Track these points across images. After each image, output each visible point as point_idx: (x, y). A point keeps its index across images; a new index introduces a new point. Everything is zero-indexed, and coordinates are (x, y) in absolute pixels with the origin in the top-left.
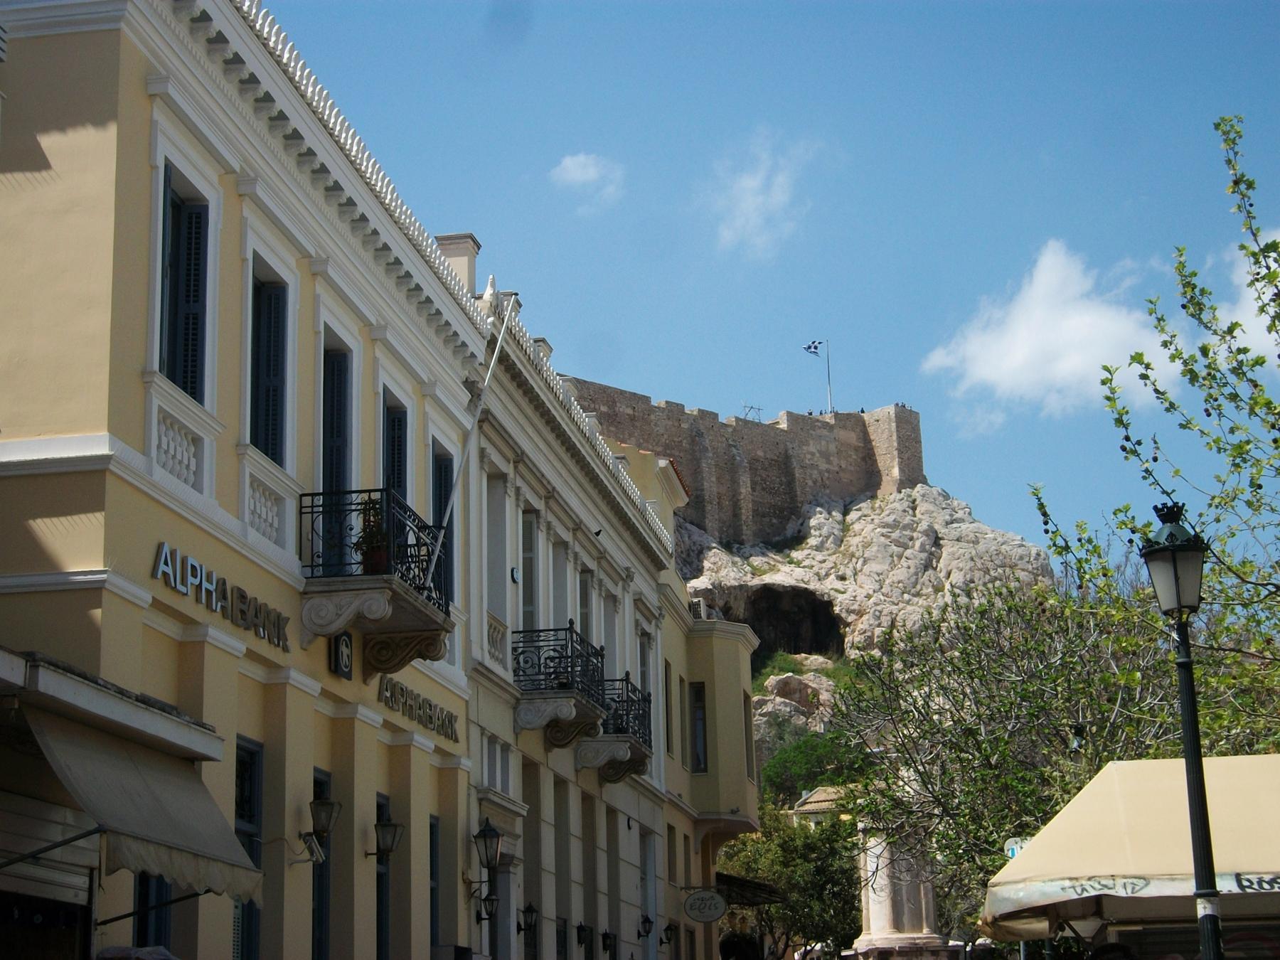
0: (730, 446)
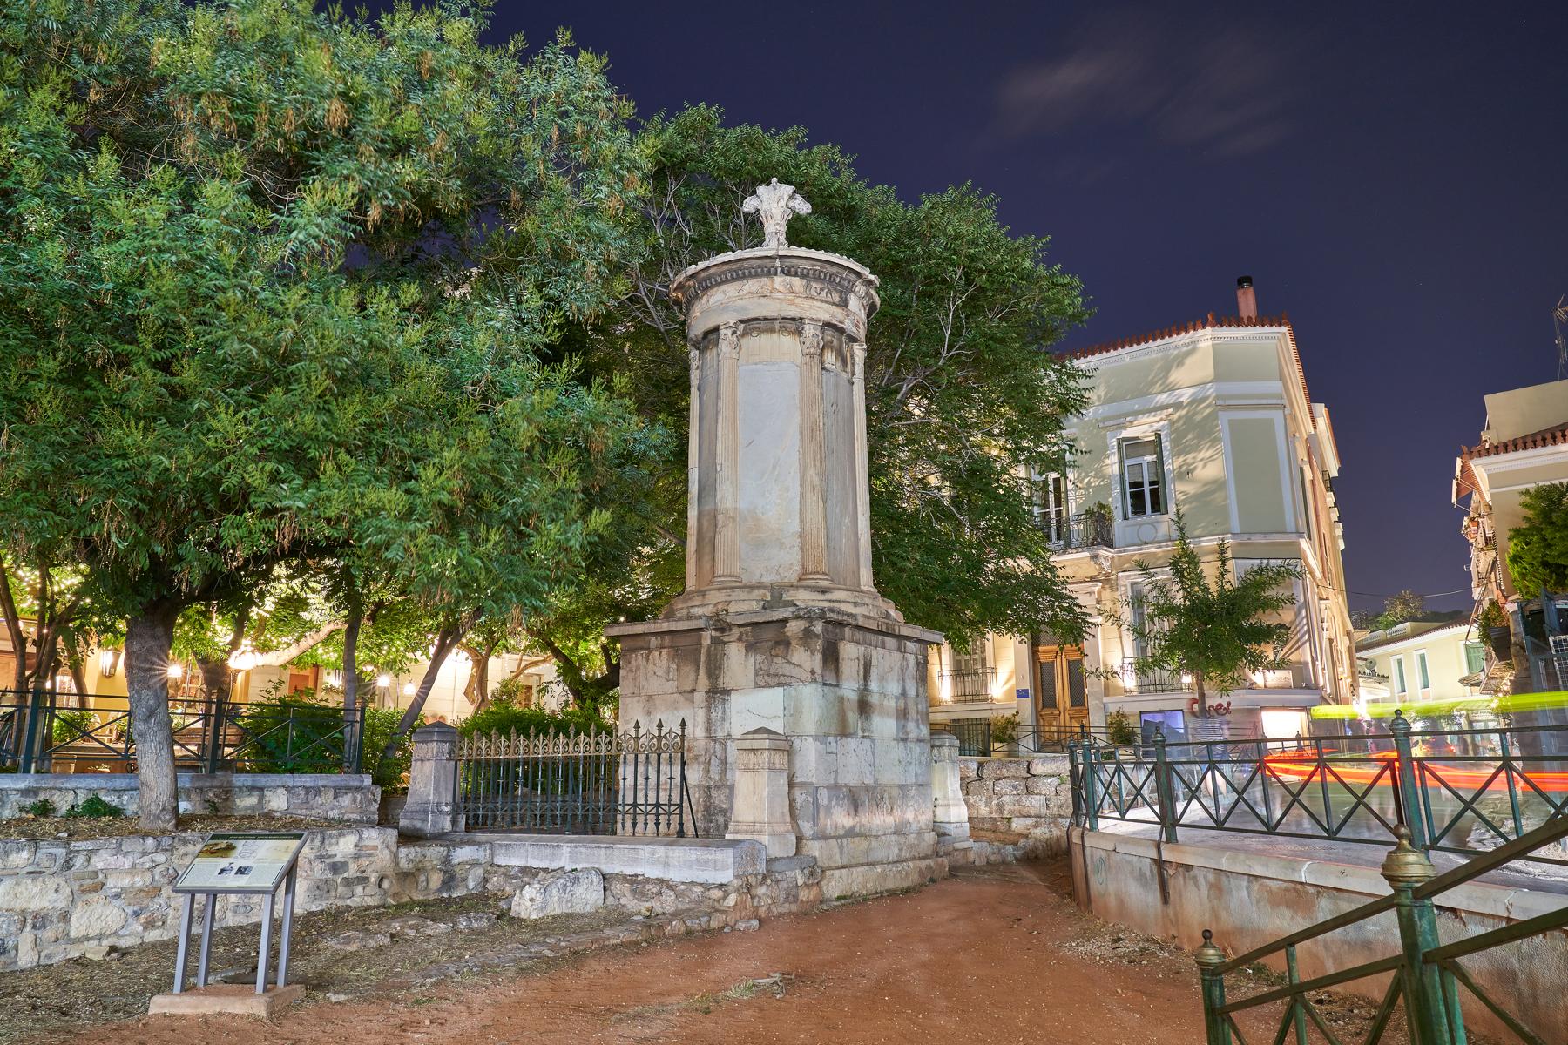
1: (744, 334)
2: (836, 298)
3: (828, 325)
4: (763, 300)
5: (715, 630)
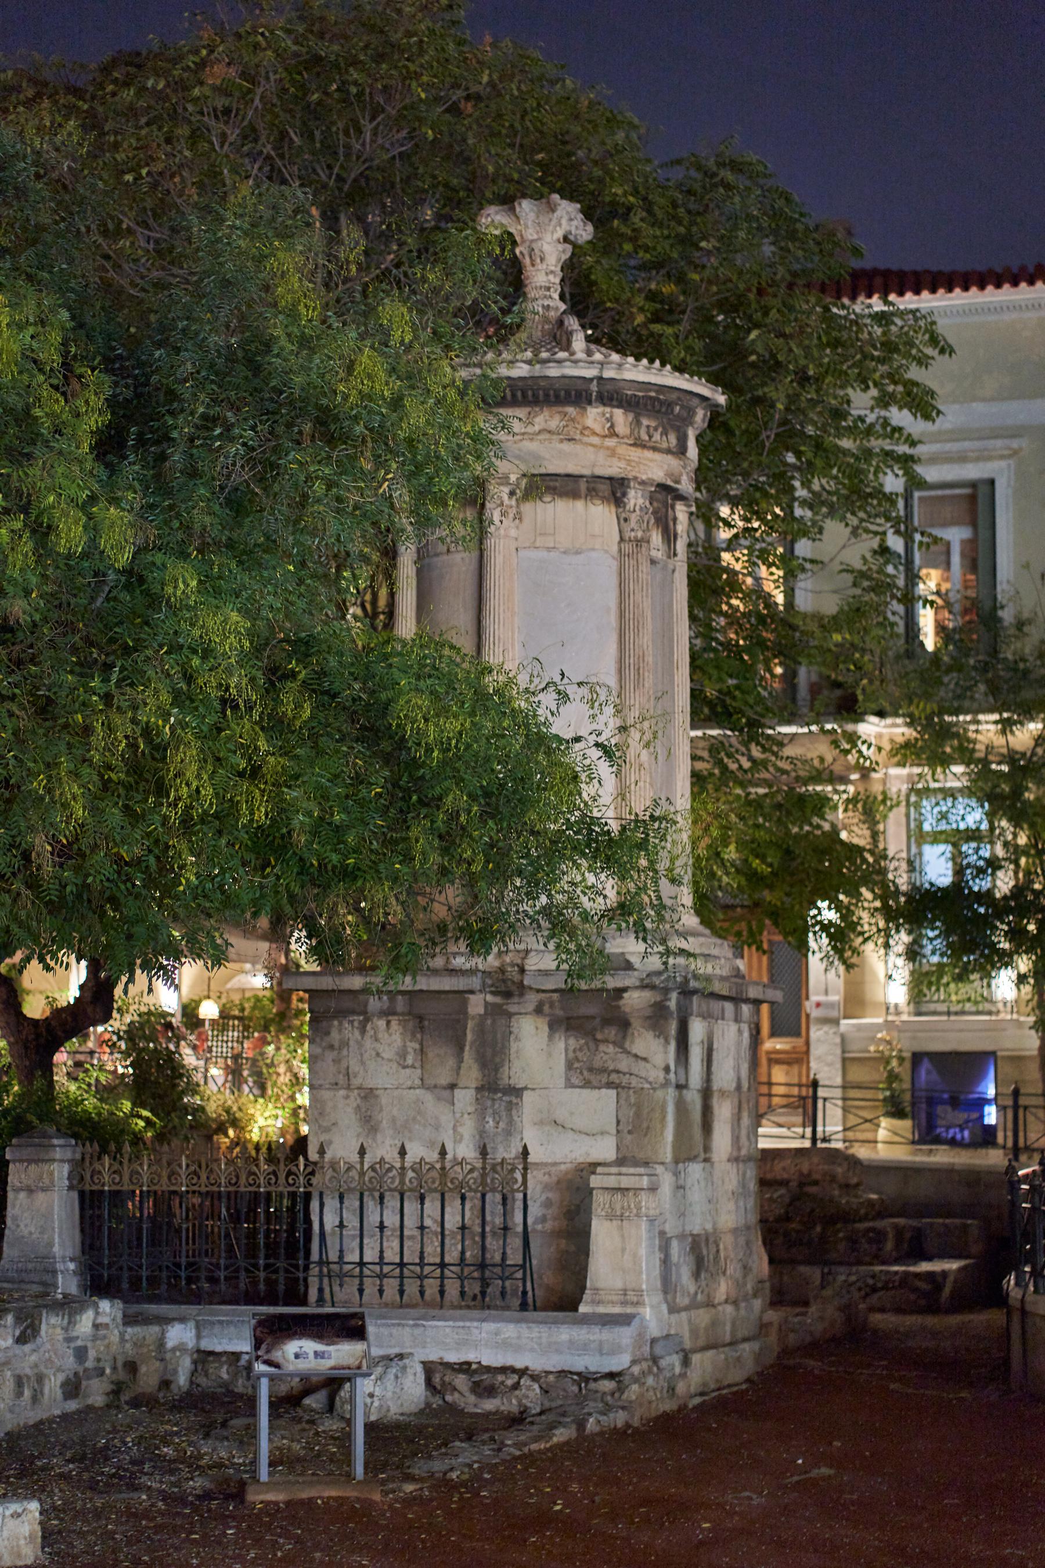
2: (673, 439)
4: (566, 447)
5: (492, 993)
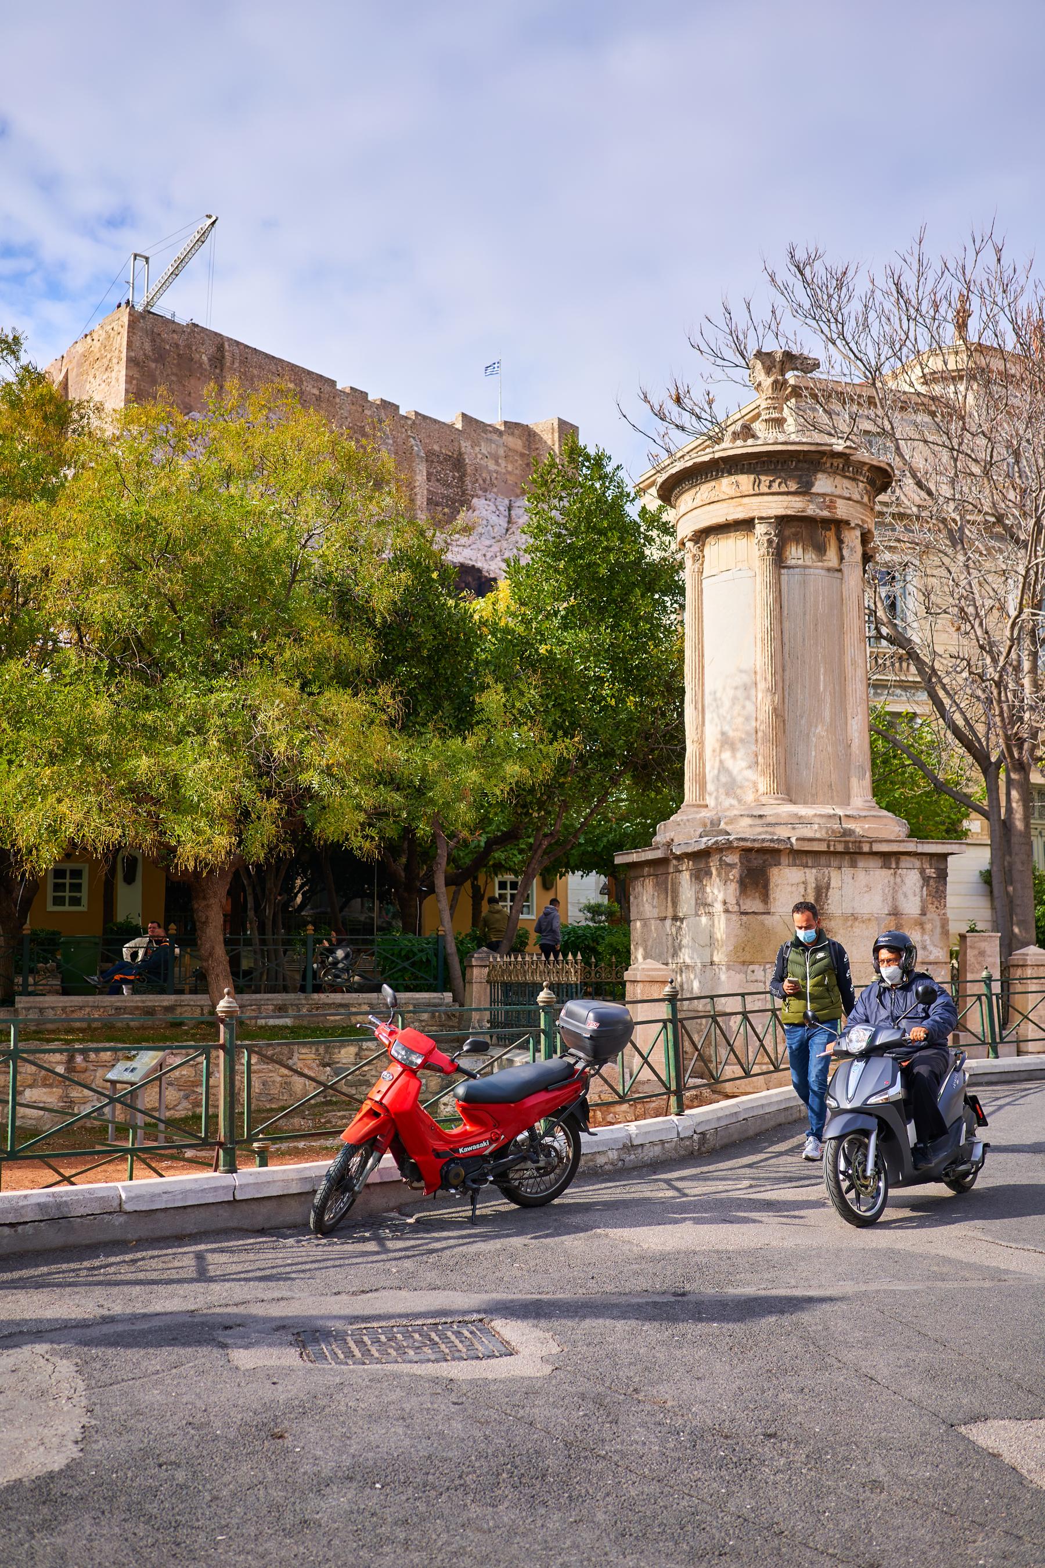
0: (410, 436)
1: (703, 545)
3: (782, 521)
